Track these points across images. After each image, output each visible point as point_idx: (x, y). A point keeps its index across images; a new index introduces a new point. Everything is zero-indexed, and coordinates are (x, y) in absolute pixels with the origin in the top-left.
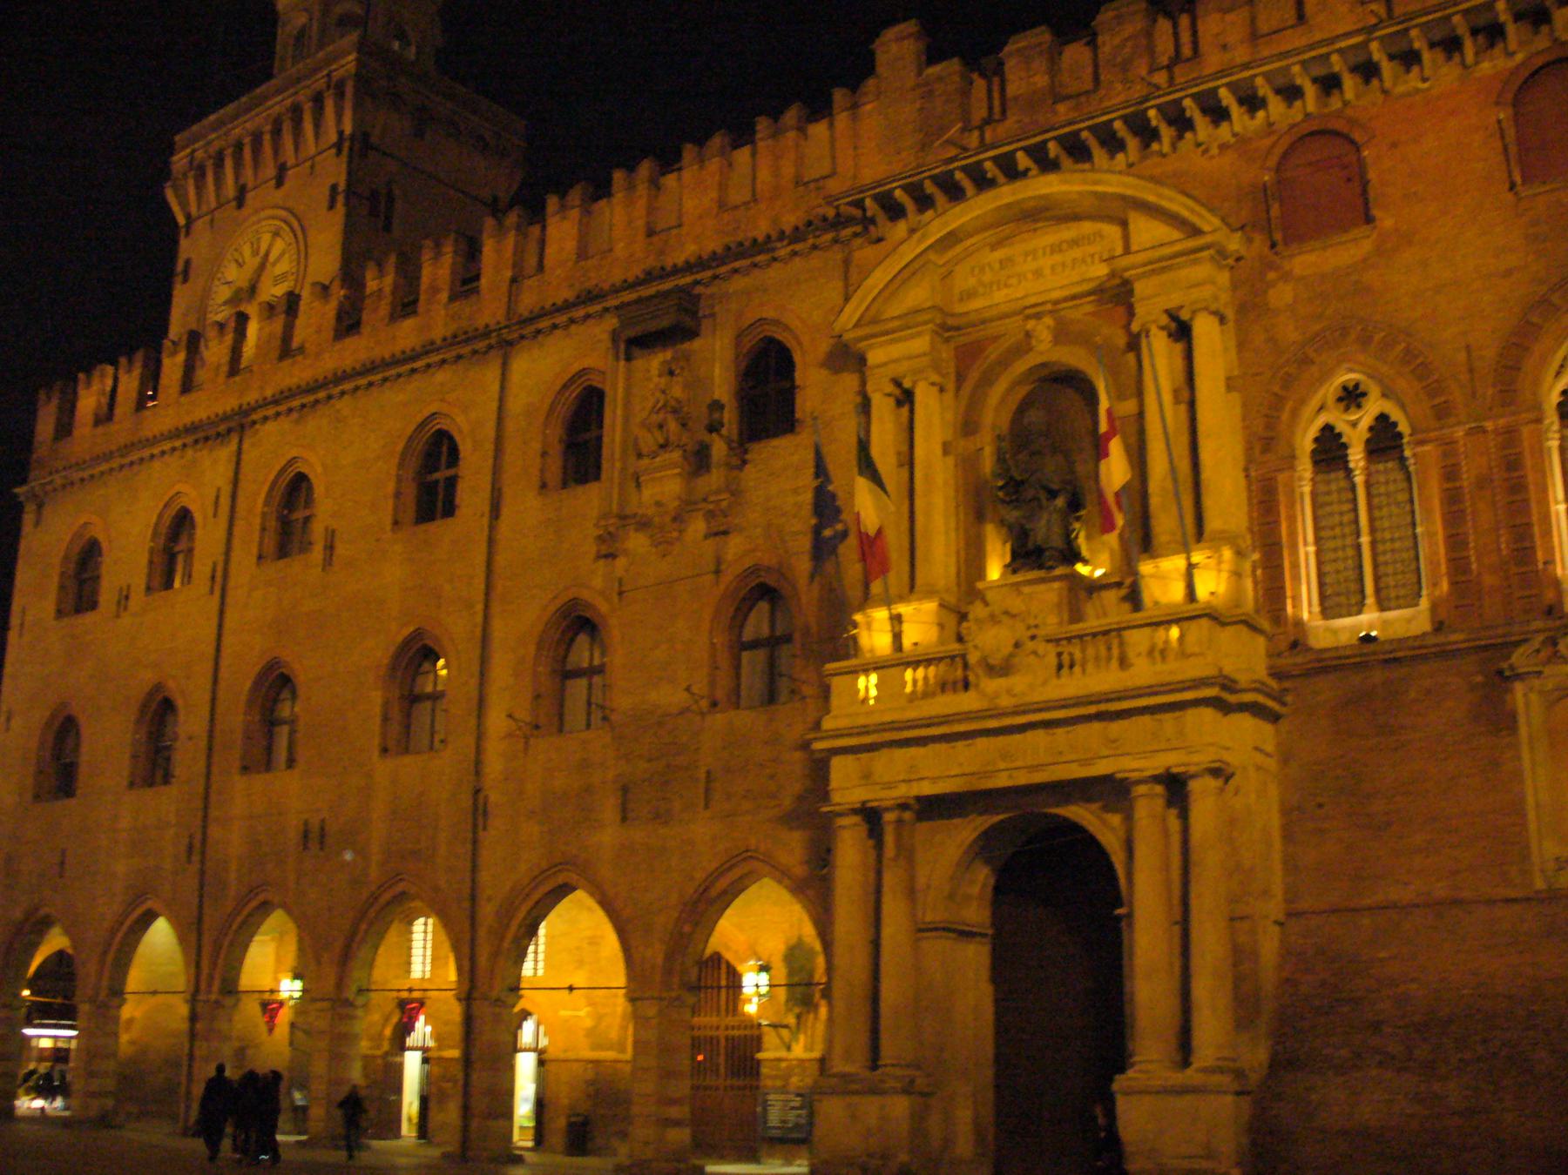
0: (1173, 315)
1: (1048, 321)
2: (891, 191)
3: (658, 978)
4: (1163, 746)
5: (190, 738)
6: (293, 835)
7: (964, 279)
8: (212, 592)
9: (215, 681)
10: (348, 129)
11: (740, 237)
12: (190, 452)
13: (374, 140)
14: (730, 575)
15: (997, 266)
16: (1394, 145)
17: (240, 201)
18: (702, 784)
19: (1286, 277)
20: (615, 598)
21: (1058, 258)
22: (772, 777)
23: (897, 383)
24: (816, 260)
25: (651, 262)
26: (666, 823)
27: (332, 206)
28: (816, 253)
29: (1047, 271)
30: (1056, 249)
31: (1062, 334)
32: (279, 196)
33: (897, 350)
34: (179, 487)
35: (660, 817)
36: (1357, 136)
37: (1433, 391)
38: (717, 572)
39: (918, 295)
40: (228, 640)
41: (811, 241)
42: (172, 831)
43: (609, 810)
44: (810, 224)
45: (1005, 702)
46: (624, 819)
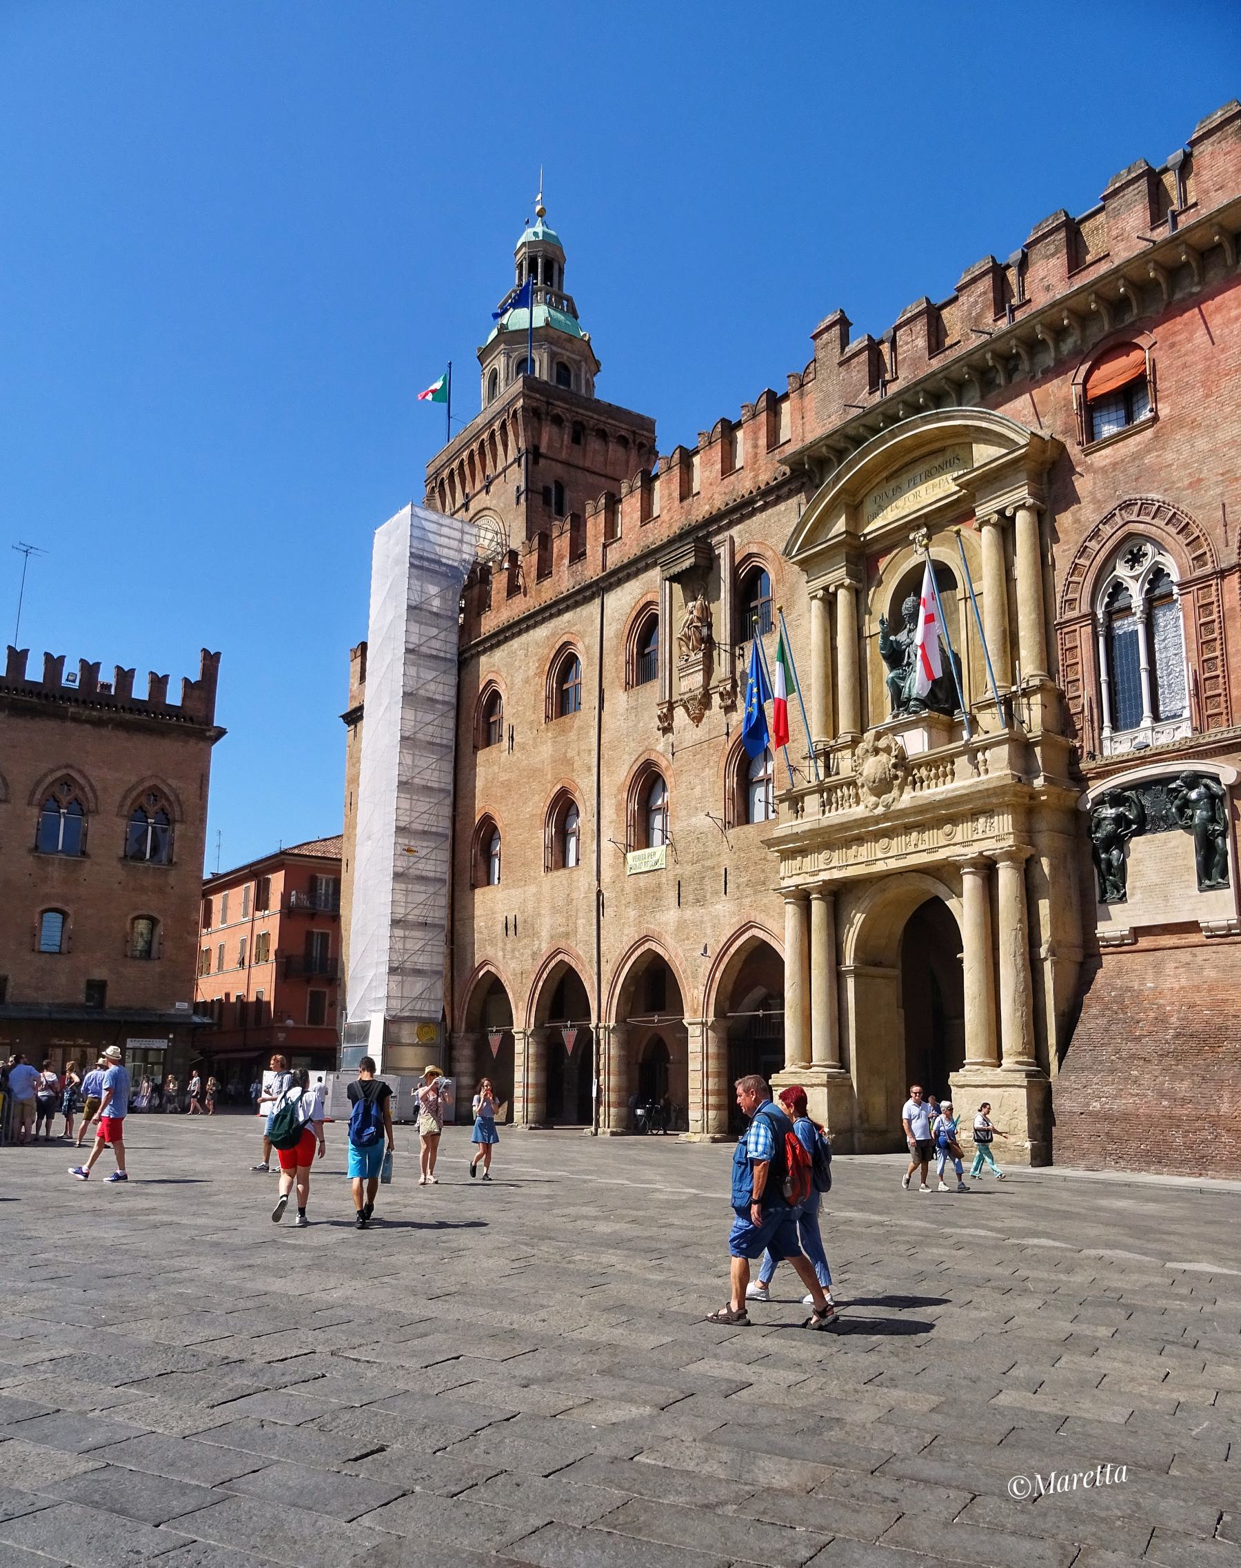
4: (981, 836)
6: (500, 928)
10: (522, 445)
13: (543, 450)
16: (1172, 345)
24: (782, 507)
27: (518, 503)
35: (700, 901)
38: (728, 734)
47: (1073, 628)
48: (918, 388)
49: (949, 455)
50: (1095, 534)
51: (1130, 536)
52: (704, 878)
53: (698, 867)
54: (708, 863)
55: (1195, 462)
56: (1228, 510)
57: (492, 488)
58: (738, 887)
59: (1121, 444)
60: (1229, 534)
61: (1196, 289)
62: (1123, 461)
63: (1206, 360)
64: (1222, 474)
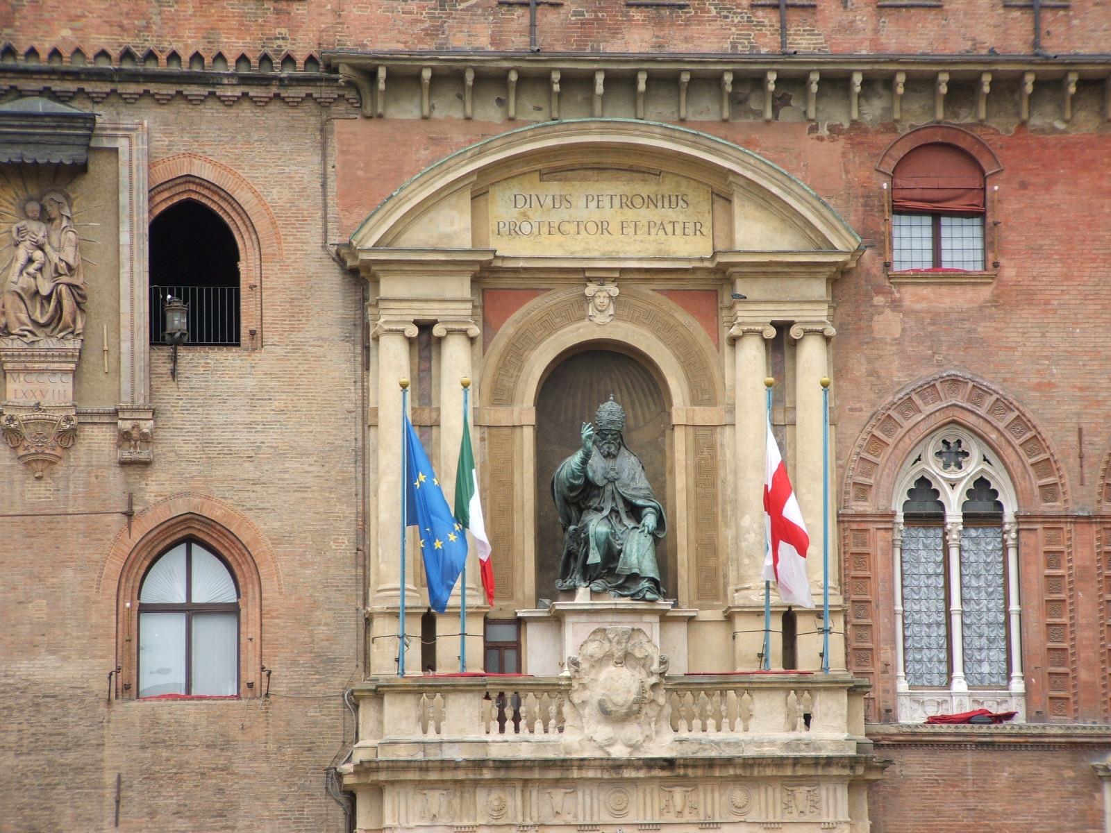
0: (782, 327)
1: (614, 290)
2: (422, 68)
7: (502, 207)
11: (150, 45)
15: (549, 201)
16: (1023, 185)
18: (110, 794)
19: (896, 305)
21: (630, 214)
23: (425, 327)
24: (276, 116)
28: (275, 106)
29: (615, 227)
30: (628, 202)
36: (985, 162)
37: (1045, 467)
38: (129, 515)
41: (274, 90)
44: (265, 59)
47: (863, 526)
48: (645, 66)
49: (668, 187)
50: (908, 405)
51: (954, 422)
52: (54, 787)
53: (36, 761)
54: (71, 758)
55: (1047, 358)
56: (1086, 438)
58: (152, 814)
59: (944, 290)
60: (1086, 470)
61: (1060, 125)
62: (946, 314)
63: (1069, 228)
64: (1081, 389)
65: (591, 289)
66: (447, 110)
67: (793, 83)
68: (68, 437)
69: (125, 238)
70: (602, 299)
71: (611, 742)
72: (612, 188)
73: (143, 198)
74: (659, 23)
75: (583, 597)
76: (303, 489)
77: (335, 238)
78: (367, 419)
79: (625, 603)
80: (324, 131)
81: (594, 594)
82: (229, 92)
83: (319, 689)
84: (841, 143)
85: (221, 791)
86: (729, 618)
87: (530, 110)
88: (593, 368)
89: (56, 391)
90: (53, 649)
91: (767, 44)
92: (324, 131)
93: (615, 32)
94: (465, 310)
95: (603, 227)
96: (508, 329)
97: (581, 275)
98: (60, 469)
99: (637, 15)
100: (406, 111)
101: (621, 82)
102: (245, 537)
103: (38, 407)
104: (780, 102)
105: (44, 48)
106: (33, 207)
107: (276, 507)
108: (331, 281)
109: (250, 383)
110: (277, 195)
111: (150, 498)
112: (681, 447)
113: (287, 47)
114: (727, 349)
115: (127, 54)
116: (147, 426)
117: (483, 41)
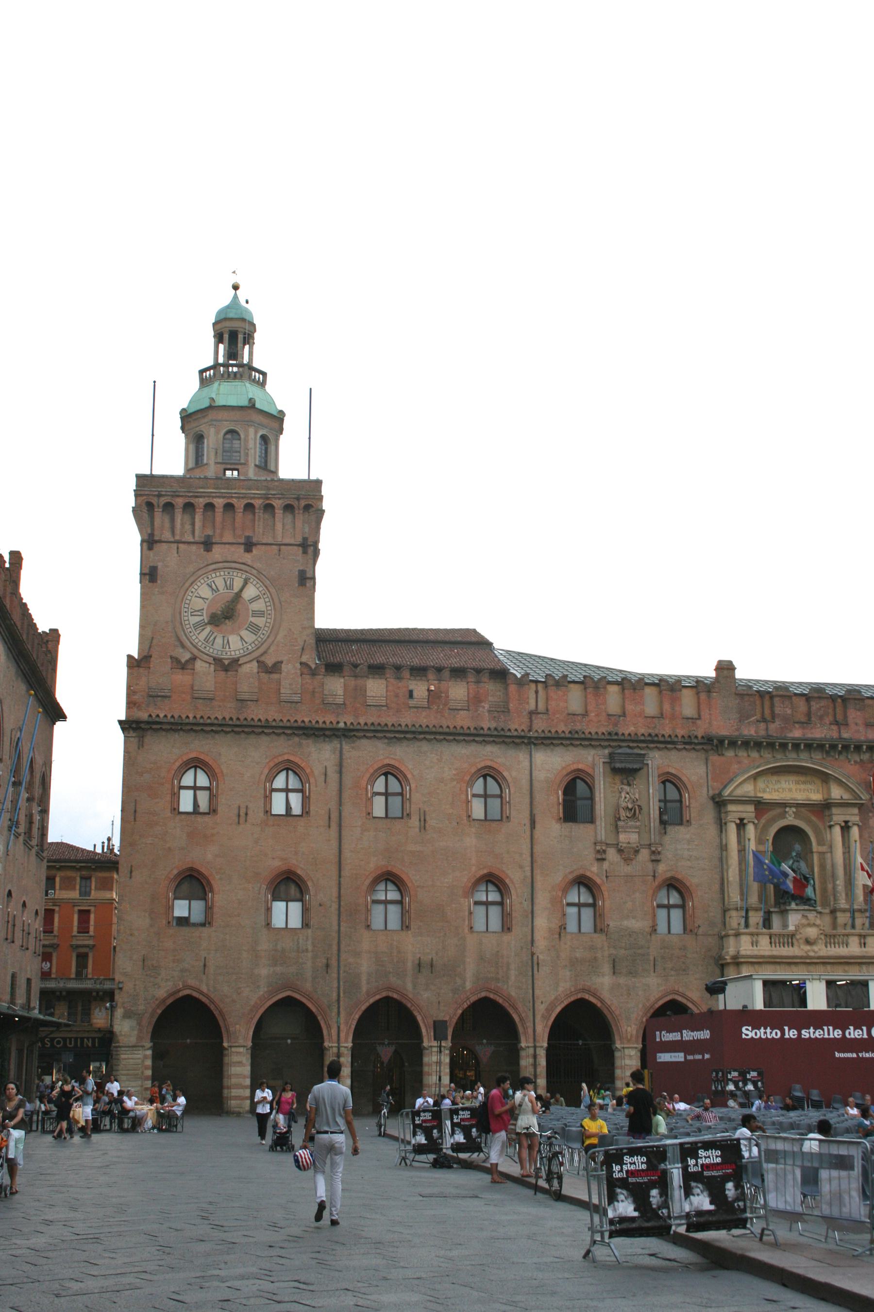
1: (794, 810)
3: (634, 1039)
5: (320, 905)
6: (409, 965)
7: (761, 783)
8: (329, 827)
9: (340, 877)
11: (657, 732)
12: (296, 739)
14: (659, 880)
17: (208, 544)
18: (652, 963)
20: (605, 879)
22: (684, 963)
23: (741, 820)
24: (693, 754)
25: (610, 728)
26: (634, 977)
29: (794, 790)
30: (797, 783)
31: (797, 815)
32: (247, 558)
33: (740, 808)
34: (292, 758)
35: (632, 973)
38: (654, 876)
39: (748, 789)
40: (347, 854)
42: (310, 955)
43: (607, 968)
45: (812, 954)
46: (614, 973)
49: (809, 778)
54: (640, 951)
57: (255, 551)
58: (664, 969)
65: (787, 809)
66: (742, 753)
67: (846, 748)
68: (637, 852)
69: (651, 791)
70: (791, 812)
71: (809, 951)
72: (792, 778)
73: (656, 779)
74: (804, 728)
75: (793, 906)
76: (704, 869)
77: (711, 793)
78: (723, 848)
79: (806, 907)
80: (707, 759)
81: (797, 905)
82: (680, 747)
83: (710, 932)
84: (857, 766)
85: (684, 963)
86: (833, 912)
87: (767, 755)
88: (789, 833)
89: (634, 837)
90: (634, 917)
91: (835, 735)
92: (707, 759)
93: (791, 731)
94: (753, 815)
95: (790, 790)
96: (763, 821)
97: (784, 805)
98: (634, 862)
99: (797, 726)
100: (730, 753)
101: (796, 746)
102: (688, 884)
103: (629, 843)
104: (840, 753)
105: (627, 733)
106: (625, 781)
107: (698, 876)
108: (711, 805)
109: (688, 836)
110: (694, 778)
111: (660, 871)
112: (816, 857)
113: (695, 733)
114: (828, 829)
115: (650, 735)
116: (659, 849)
117: (753, 732)
